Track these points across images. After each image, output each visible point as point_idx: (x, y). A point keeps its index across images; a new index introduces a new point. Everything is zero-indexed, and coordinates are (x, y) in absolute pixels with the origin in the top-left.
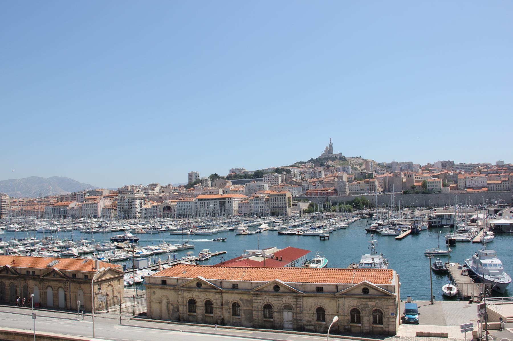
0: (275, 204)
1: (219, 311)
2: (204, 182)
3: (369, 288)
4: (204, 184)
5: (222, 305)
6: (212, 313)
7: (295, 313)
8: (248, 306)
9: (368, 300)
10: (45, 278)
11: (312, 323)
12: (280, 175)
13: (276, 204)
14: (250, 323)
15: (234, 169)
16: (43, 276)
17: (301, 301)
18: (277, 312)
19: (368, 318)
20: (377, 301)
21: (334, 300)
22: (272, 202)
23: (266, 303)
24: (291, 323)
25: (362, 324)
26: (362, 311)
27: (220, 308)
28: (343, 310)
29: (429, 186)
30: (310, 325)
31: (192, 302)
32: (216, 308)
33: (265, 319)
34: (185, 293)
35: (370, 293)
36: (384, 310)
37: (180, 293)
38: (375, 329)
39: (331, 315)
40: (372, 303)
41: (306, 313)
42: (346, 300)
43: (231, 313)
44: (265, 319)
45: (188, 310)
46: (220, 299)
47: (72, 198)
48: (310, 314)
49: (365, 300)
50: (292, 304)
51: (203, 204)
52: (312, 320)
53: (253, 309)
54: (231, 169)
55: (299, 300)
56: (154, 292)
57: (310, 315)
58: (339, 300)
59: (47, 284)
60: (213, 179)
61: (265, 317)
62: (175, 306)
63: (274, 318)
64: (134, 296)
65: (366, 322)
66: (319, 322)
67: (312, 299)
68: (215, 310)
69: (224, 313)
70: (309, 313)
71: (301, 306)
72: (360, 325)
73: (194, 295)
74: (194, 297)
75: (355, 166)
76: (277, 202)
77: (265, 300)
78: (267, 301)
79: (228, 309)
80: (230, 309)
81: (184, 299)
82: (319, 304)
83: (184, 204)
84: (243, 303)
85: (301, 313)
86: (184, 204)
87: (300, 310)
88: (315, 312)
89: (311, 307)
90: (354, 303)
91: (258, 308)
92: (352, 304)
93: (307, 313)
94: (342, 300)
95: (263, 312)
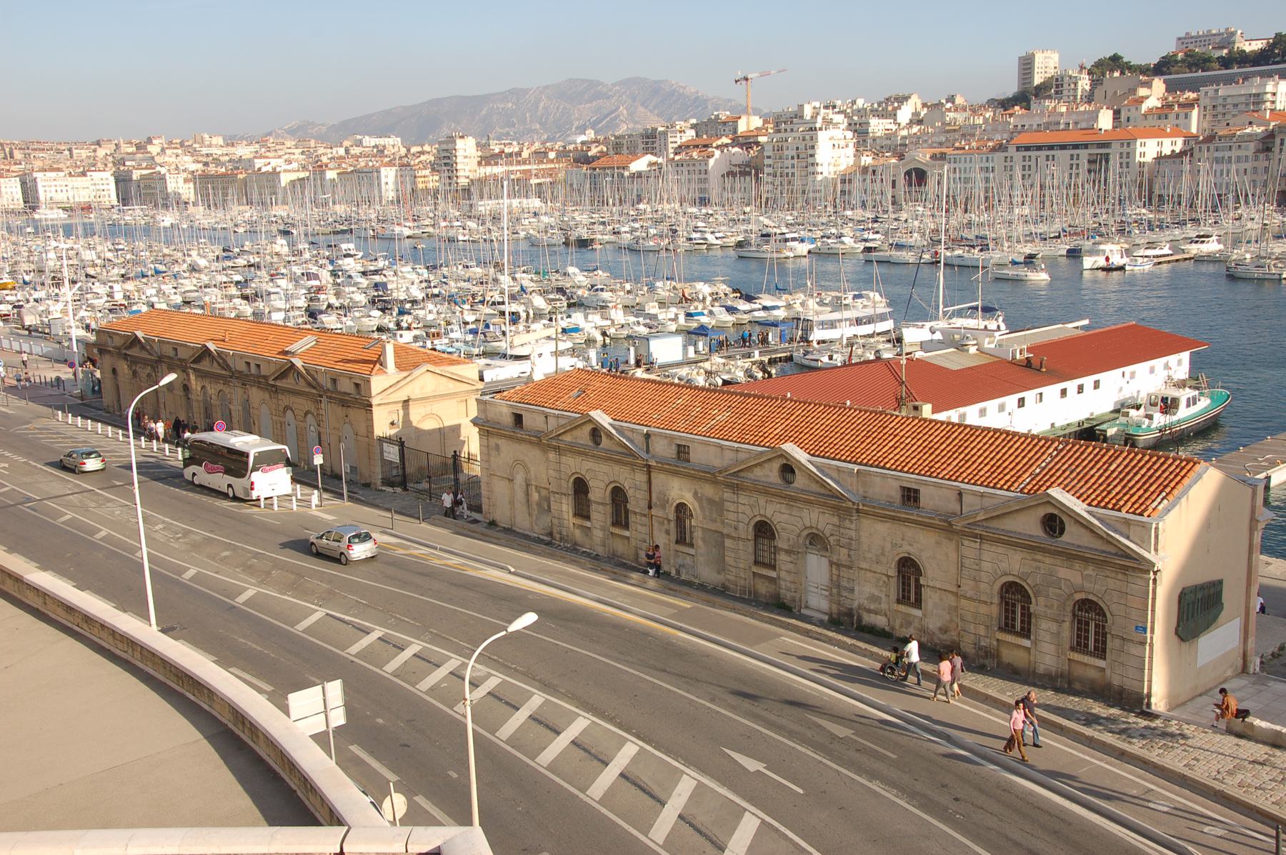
3: (1064, 518)
4: (1065, 93)
5: (650, 507)
6: (626, 526)
7: (835, 564)
8: (714, 521)
9: (1058, 562)
11: (884, 606)
14: (719, 573)
15: (1194, 34)
16: (275, 379)
17: (853, 526)
18: (788, 552)
19: (1054, 627)
20: (1090, 571)
21: (951, 540)
23: (758, 519)
24: (827, 593)
25: (1035, 643)
26: (1036, 597)
27: (645, 516)
28: (974, 579)
31: (581, 487)
32: (635, 513)
34: (564, 459)
36: (1113, 607)
37: (552, 456)
38: (1078, 671)
40: (1071, 575)
42: (985, 546)
43: (673, 537)
44: (755, 569)
46: (645, 487)
47: (647, 143)
48: (878, 575)
49: (1048, 560)
50: (827, 533)
51: (1033, 163)
53: (725, 531)
54: (1183, 35)
55: (847, 523)
56: (497, 447)
57: (878, 580)
58: (966, 543)
59: (285, 400)
61: (756, 563)
62: (544, 493)
63: (780, 569)
64: (455, 452)
65: (1048, 638)
66: (902, 608)
67: (887, 525)
68: (632, 518)
69: (656, 533)
71: (850, 544)
72: (1026, 643)
80: (669, 521)
81: (563, 477)
82: (906, 548)
88: (893, 572)
89: (883, 554)
90: (1014, 564)
92: (1004, 566)
93: (870, 571)
94: (973, 545)
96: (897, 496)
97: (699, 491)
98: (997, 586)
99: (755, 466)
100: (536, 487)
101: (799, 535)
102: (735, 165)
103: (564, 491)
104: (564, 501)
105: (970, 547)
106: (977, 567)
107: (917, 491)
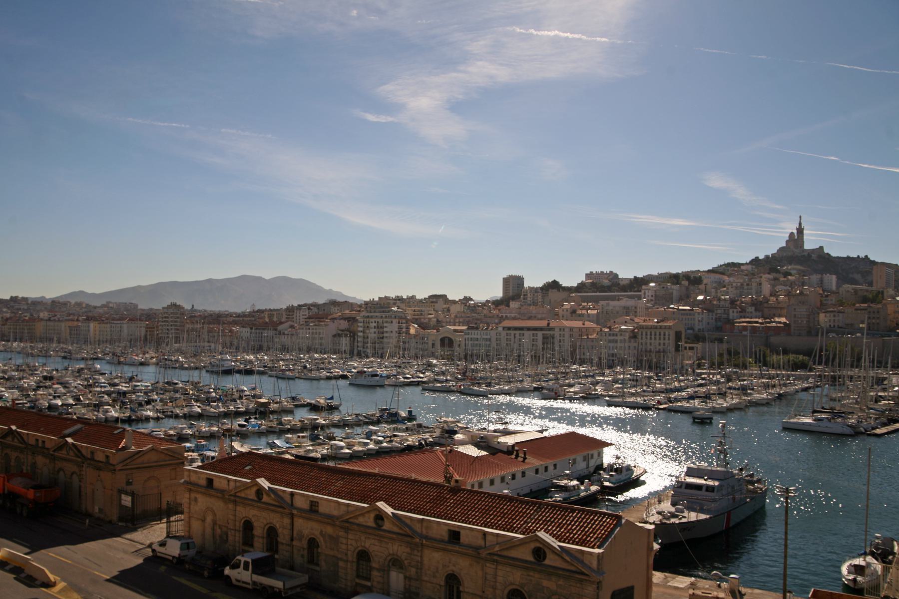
0: (649, 344)
2: (529, 295)
3: (547, 550)
4: (529, 299)
5: (292, 540)
10: (56, 454)
13: (651, 344)
17: (419, 554)
18: (378, 570)
22: (662, 342)
23: (360, 548)
27: (288, 545)
31: (248, 526)
32: (282, 544)
33: (357, 581)
34: (238, 508)
35: (547, 562)
39: (472, 594)
41: (426, 581)
42: (500, 567)
44: (357, 581)
45: (241, 541)
46: (289, 527)
47: (289, 315)
49: (537, 576)
50: (403, 558)
51: (512, 337)
53: (340, 556)
54: (589, 273)
55: (416, 552)
56: (196, 500)
58: (488, 565)
60: (548, 290)
61: (358, 576)
62: (224, 529)
63: (373, 581)
67: (440, 553)
68: (280, 547)
70: (432, 583)
71: (418, 565)
73: (251, 513)
74: (250, 517)
76: (653, 341)
78: (363, 544)
79: (302, 550)
80: (304, 549)
81: (237, 519)
82: (452, 568)
83: (477, 334)
85: (417, 580)
86: (477, 334)
87: (417, 573)
88: (443, 583)
91: (346, 554)
95: (355, 565)
96: (446, 536)
97: (324, 530)
98: (506, 592)
99: (359, 515)
100: (219, 526)
101: (385, 559)
102: (340, 330)
103: (237, 528)
104: (237, 534)
105: (490, 568)
106: (494, 580)
107: (459, 533)
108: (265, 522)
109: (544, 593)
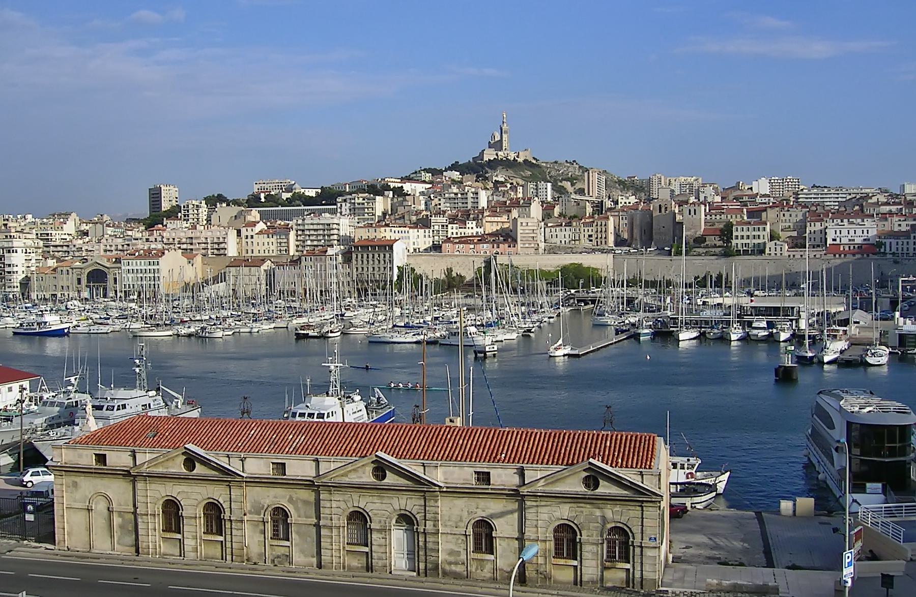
1: (237, 529)
12: (379, 199)
18: (379, 531)
20: (617, 508)
23: (351, 510)
29: (737, 237)
30: (456, 563)
43: (269, 534)
48: (457, 536)
50: (414, 512)
52: (461, 550)
56: (75, 484)
65: (589, 556)
75: (560, 184)
77: (349, 501)
84: (297, 509)
87: (434, 526)
88: (470, 531)
89: (461, 520)
90: (564, 512)
92: (557, 514)
98: (551, 529)
108: (200, 498)
109: (598, 523)
